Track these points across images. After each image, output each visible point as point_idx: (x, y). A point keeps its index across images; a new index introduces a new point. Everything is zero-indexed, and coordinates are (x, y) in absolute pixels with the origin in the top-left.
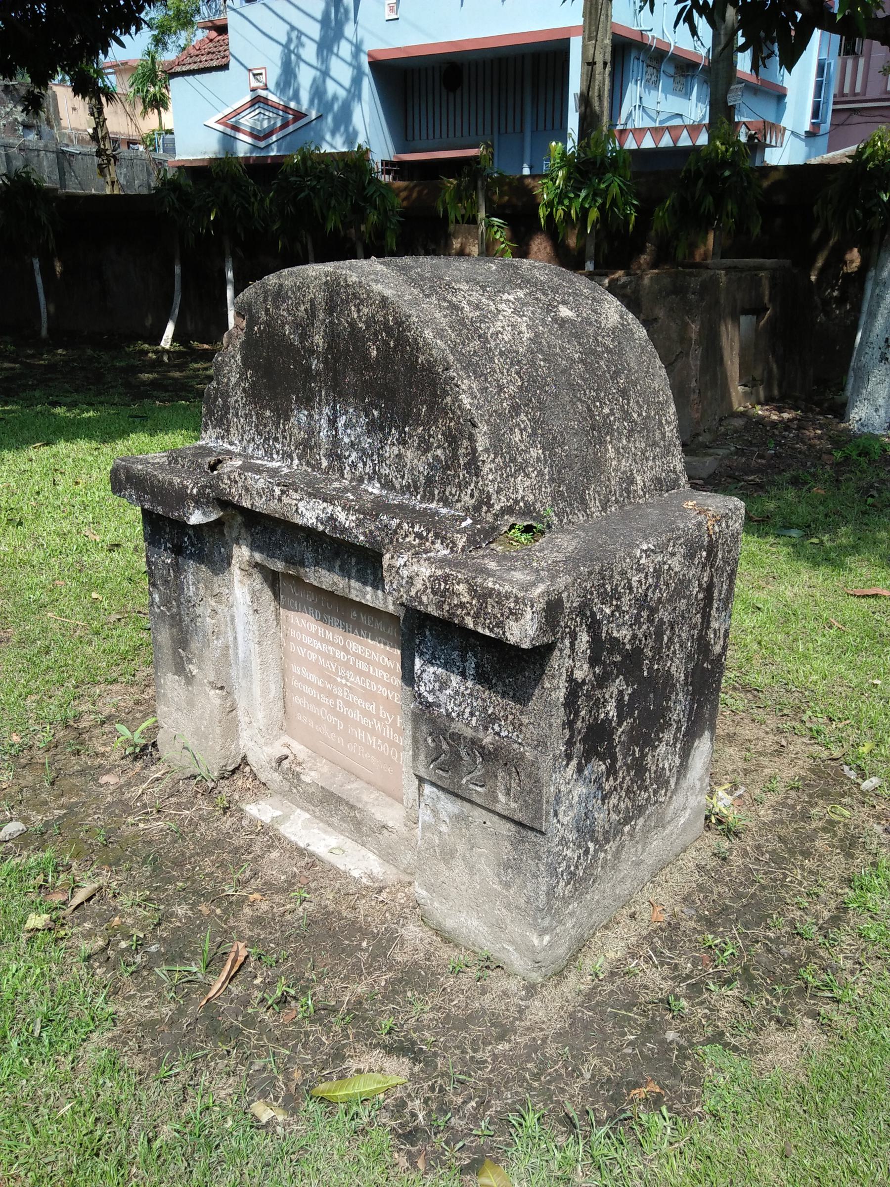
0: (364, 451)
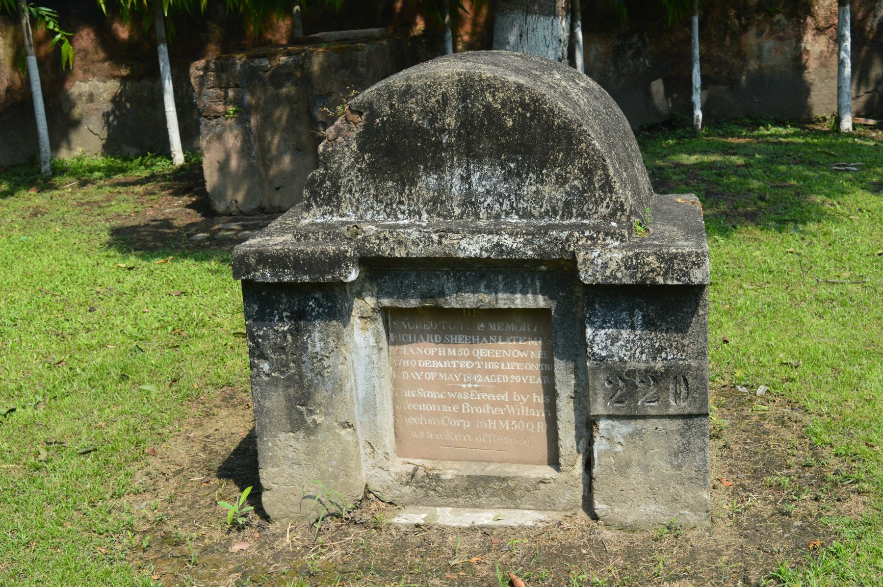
0: (500, 195)
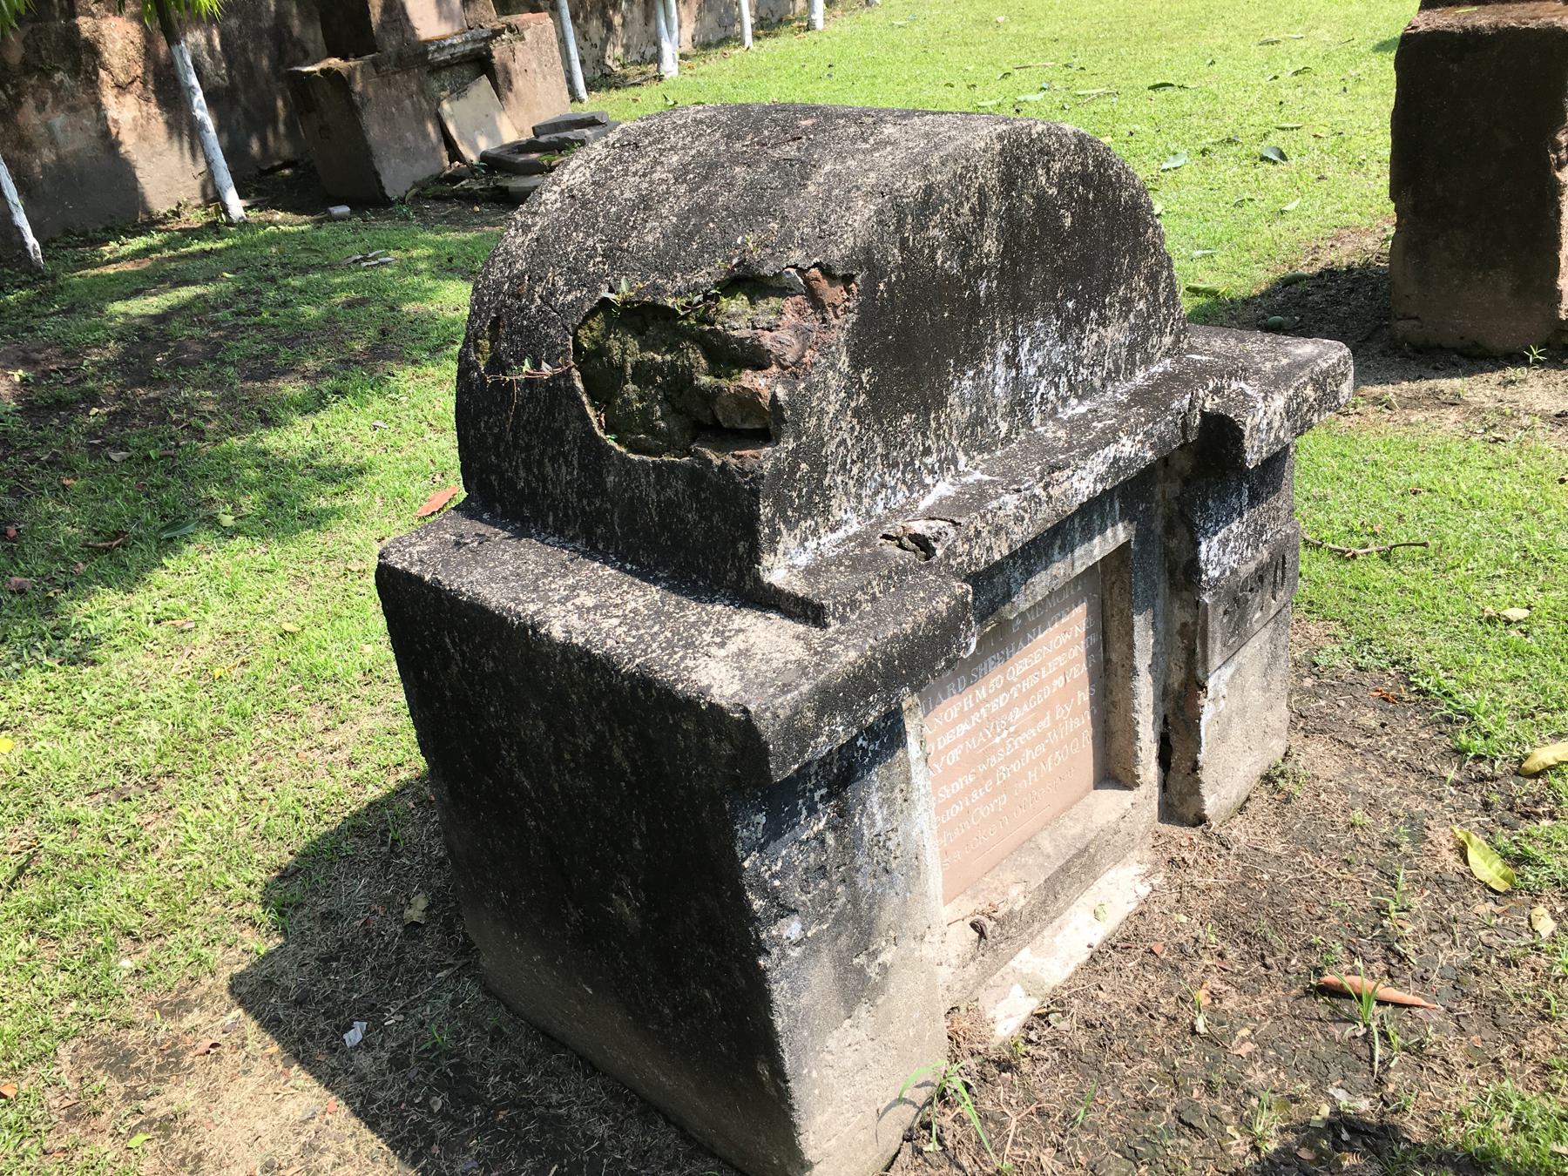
0: (1057, 371)
